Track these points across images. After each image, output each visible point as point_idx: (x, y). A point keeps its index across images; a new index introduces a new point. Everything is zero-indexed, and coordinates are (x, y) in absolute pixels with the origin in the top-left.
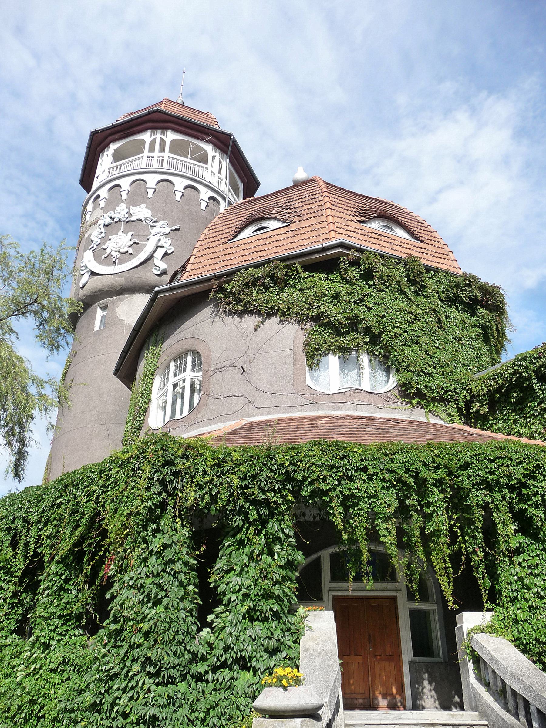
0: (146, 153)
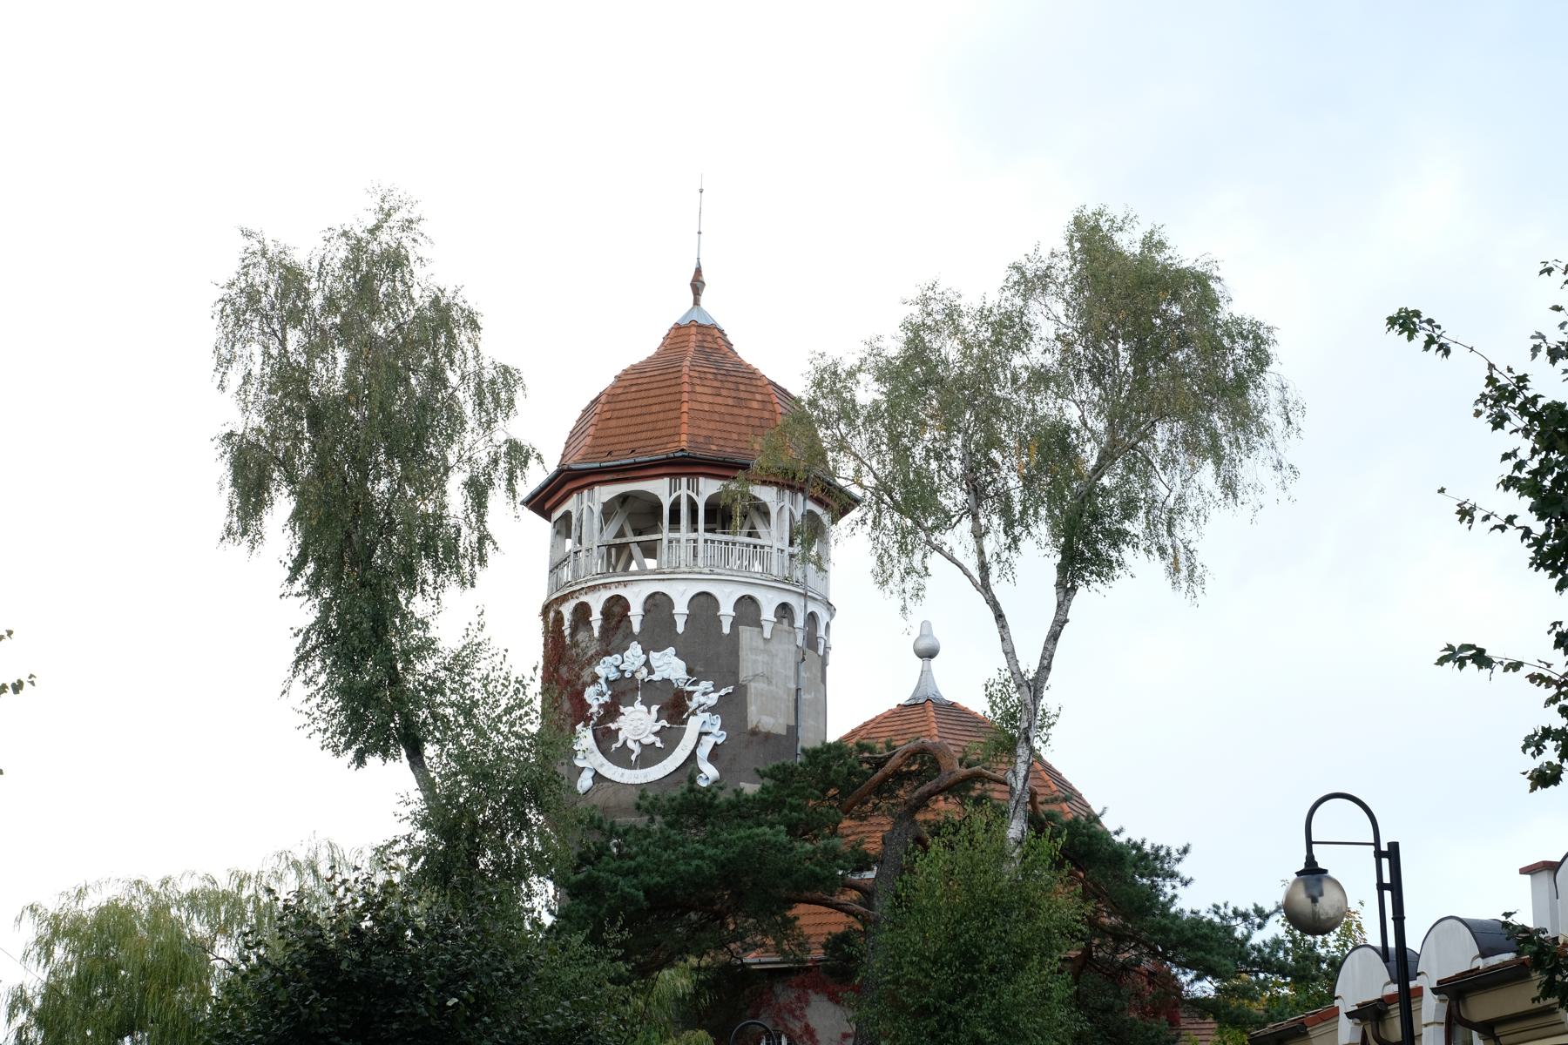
0: (665, 534)
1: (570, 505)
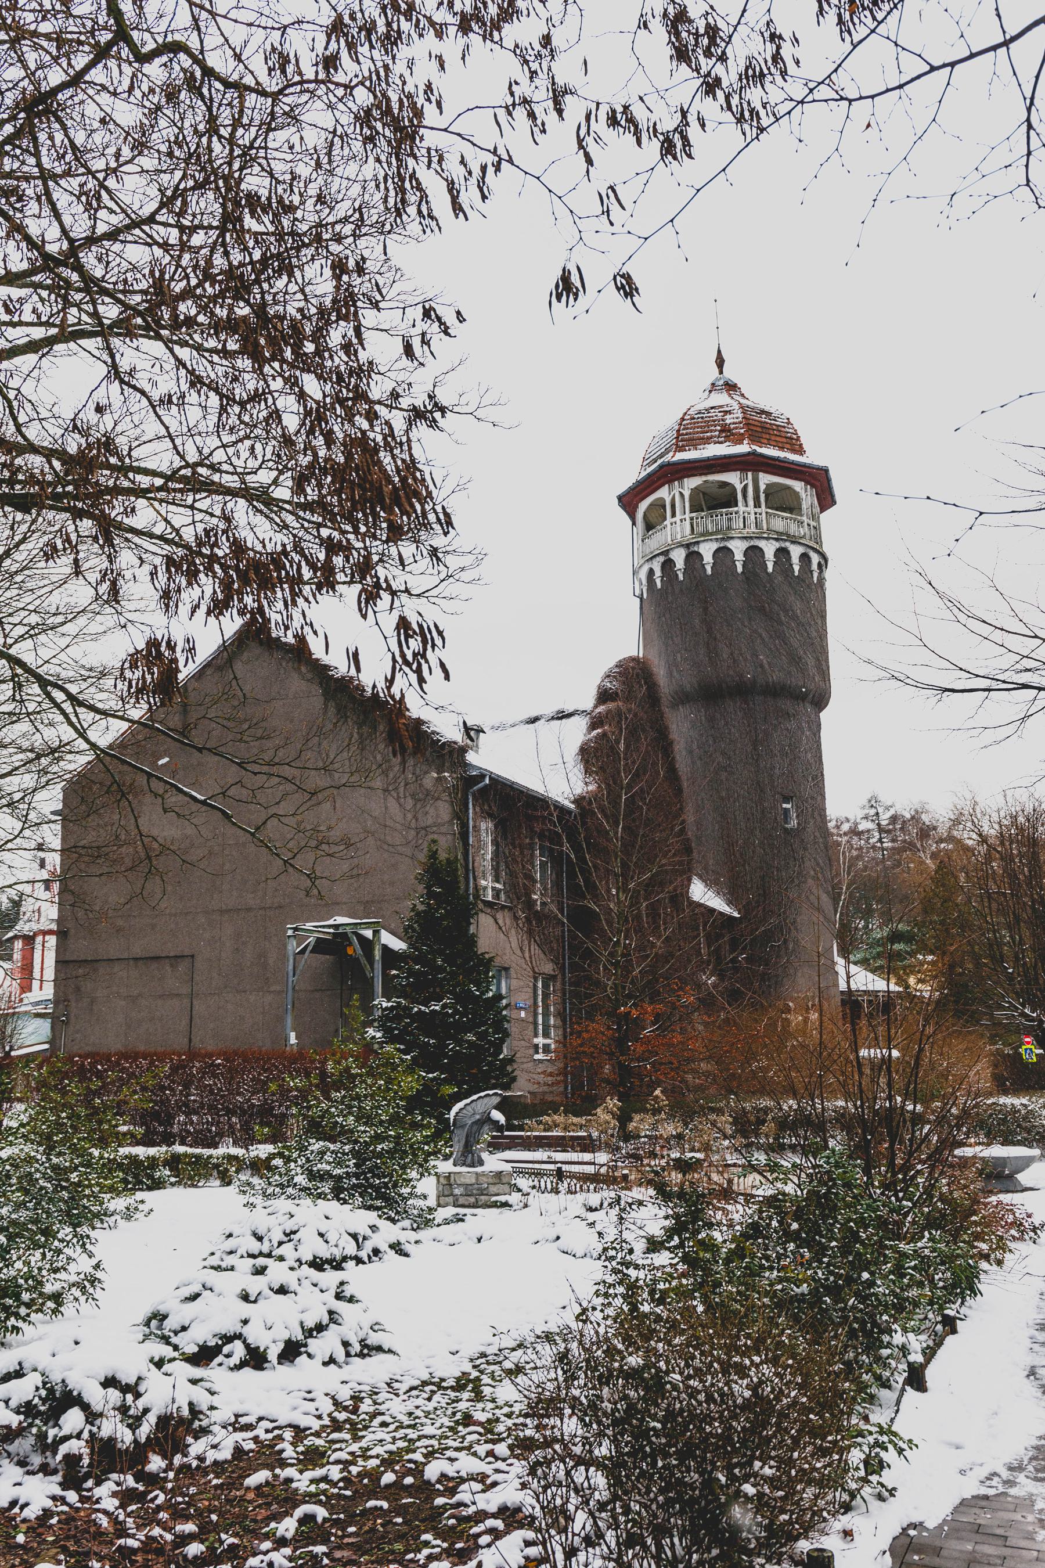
0: (741, 507)
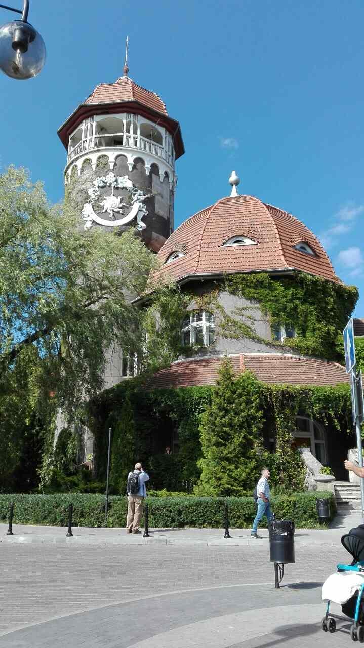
1: (83, 126)
